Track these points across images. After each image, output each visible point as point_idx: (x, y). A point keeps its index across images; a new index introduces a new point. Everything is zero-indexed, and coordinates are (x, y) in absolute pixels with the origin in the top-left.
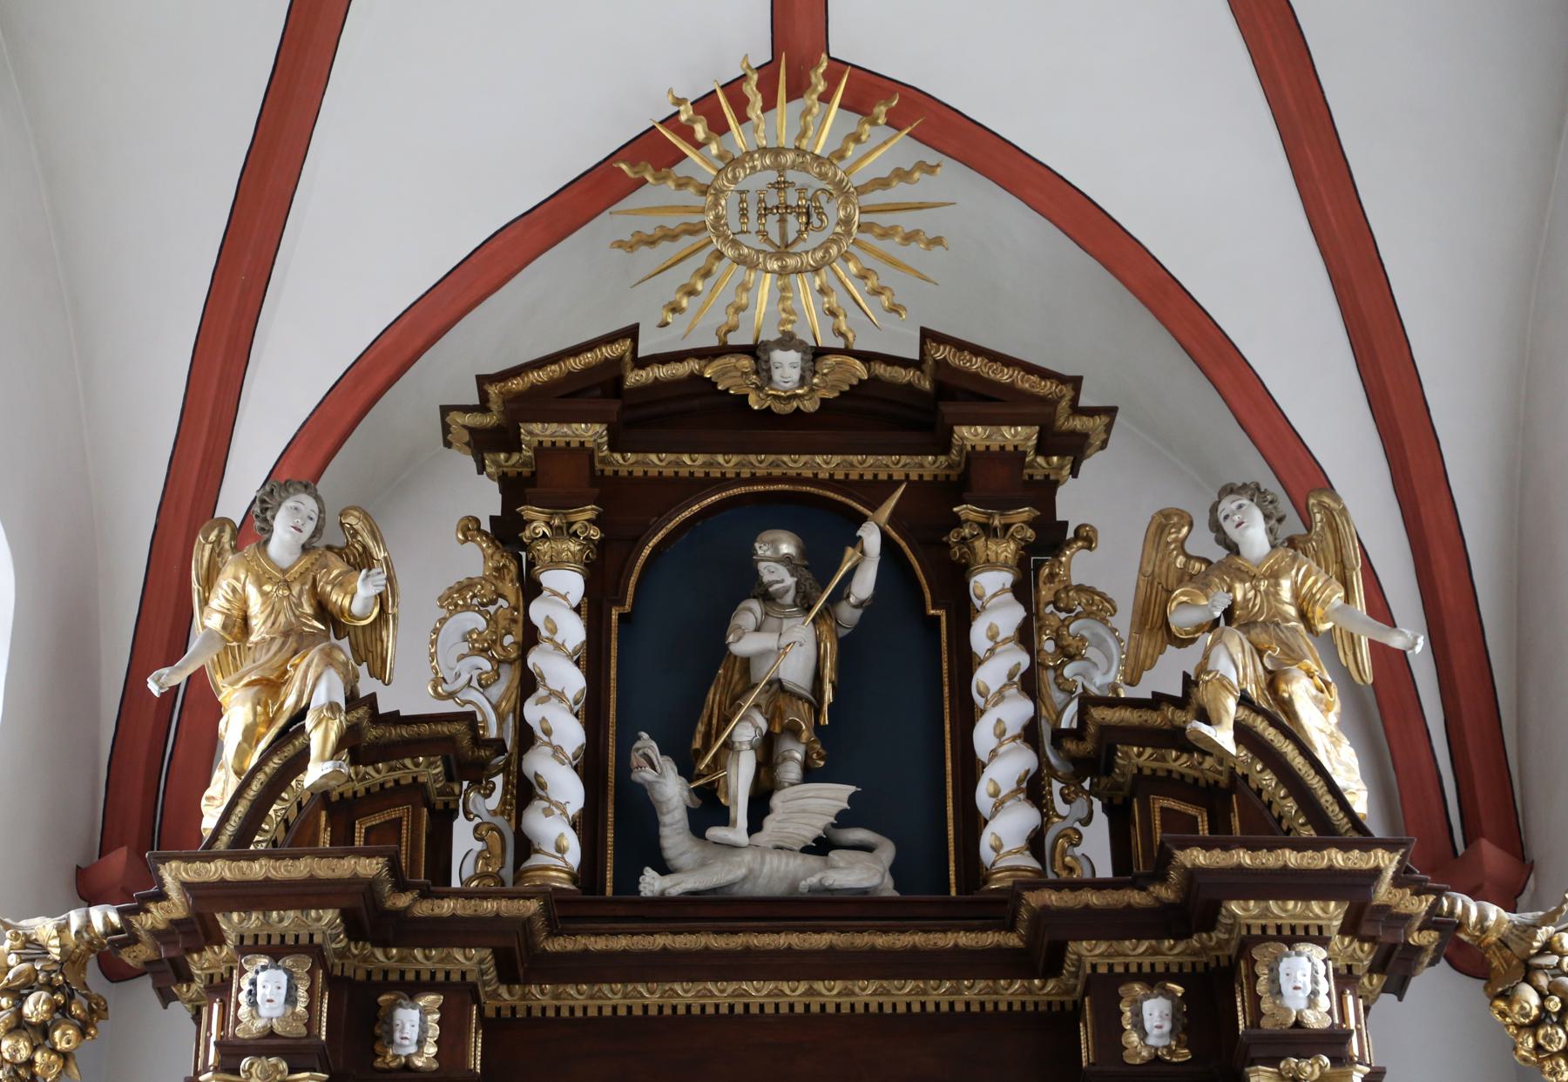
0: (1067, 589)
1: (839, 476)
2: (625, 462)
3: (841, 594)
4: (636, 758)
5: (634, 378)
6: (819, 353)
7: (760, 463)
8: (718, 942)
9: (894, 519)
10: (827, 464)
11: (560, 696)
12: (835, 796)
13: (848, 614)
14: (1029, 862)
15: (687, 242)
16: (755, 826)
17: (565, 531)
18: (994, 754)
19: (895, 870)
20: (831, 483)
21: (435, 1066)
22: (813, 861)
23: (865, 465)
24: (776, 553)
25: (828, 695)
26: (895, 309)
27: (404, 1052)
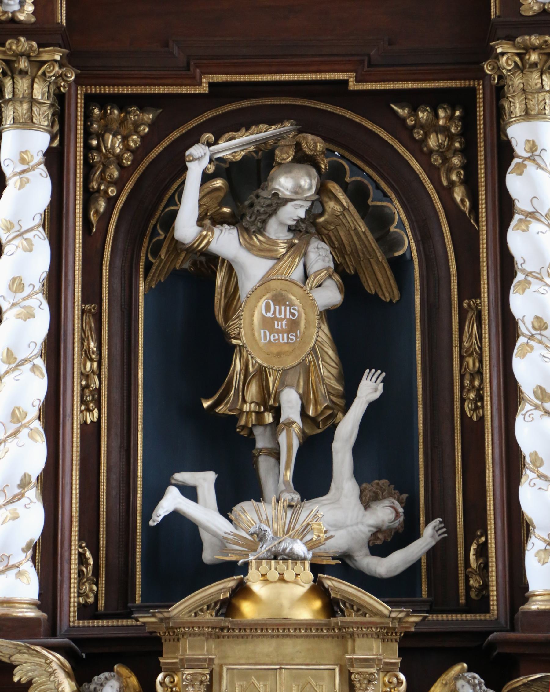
21: (33, 19)
27: (11, 9)
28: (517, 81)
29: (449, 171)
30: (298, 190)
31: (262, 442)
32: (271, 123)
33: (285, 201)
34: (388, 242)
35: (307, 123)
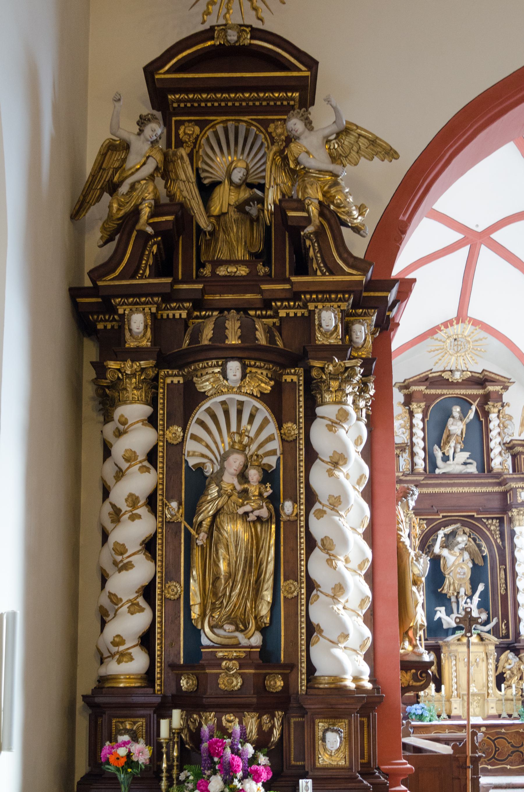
0: (505, 415)
1: (465, 393)
2: (428, 392)
3: (468, 418)
4: (435, 450)
5: (430, 376)
6: (463, 371)
7: (451, 391)
8: (449, 482)
9: (477, 405)
10: (463, 392)
11: (420, 437)
12: (467, 454)
13: (468, 421)
14: (500, 467)
15: (440, 351)
16: (453, 460)
17: (420, 407)
18: (494, 448)
19: (477, 467)
20: (463, 395)
22: (464, 467)
23: (469, 392)
24: (456, 410)
25: (464, 436)
26: (476, 363)
28: (517, 517)
29: (496, 535)
30: (463, 541)
31: (453, 599)
32: (455, 524)
33: (460, 543)
34: (481, 551)
35: (464, 524)
